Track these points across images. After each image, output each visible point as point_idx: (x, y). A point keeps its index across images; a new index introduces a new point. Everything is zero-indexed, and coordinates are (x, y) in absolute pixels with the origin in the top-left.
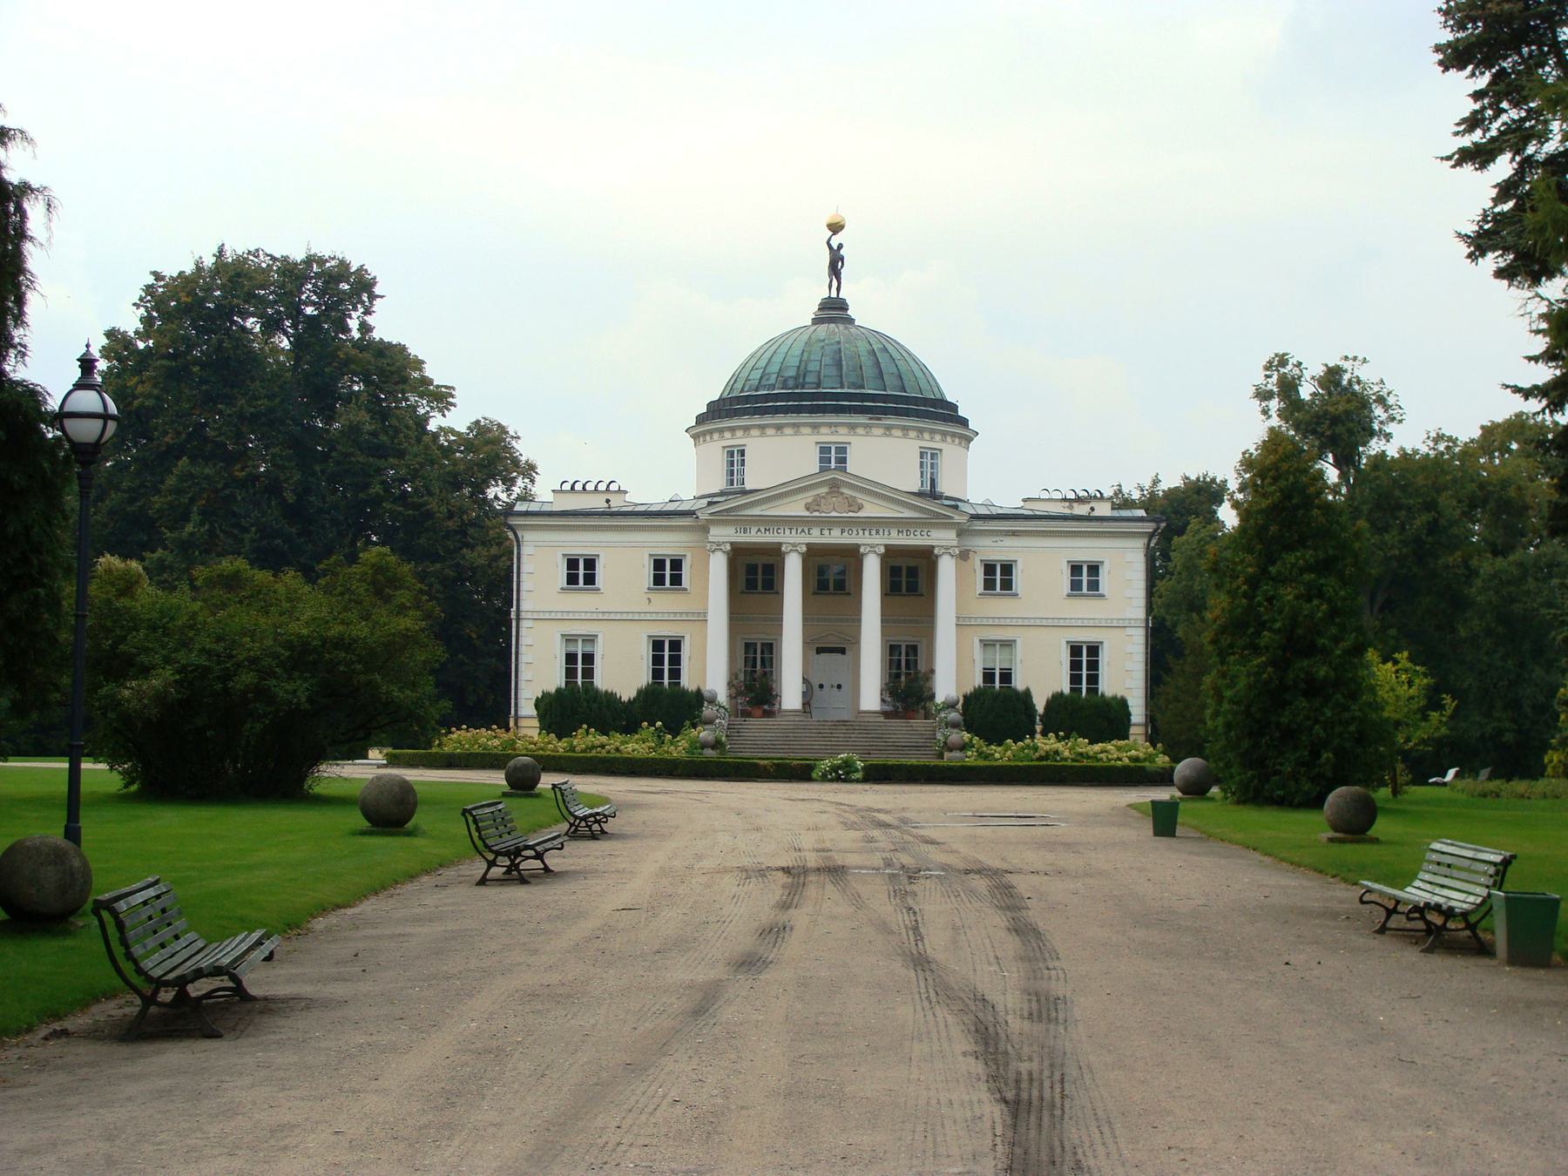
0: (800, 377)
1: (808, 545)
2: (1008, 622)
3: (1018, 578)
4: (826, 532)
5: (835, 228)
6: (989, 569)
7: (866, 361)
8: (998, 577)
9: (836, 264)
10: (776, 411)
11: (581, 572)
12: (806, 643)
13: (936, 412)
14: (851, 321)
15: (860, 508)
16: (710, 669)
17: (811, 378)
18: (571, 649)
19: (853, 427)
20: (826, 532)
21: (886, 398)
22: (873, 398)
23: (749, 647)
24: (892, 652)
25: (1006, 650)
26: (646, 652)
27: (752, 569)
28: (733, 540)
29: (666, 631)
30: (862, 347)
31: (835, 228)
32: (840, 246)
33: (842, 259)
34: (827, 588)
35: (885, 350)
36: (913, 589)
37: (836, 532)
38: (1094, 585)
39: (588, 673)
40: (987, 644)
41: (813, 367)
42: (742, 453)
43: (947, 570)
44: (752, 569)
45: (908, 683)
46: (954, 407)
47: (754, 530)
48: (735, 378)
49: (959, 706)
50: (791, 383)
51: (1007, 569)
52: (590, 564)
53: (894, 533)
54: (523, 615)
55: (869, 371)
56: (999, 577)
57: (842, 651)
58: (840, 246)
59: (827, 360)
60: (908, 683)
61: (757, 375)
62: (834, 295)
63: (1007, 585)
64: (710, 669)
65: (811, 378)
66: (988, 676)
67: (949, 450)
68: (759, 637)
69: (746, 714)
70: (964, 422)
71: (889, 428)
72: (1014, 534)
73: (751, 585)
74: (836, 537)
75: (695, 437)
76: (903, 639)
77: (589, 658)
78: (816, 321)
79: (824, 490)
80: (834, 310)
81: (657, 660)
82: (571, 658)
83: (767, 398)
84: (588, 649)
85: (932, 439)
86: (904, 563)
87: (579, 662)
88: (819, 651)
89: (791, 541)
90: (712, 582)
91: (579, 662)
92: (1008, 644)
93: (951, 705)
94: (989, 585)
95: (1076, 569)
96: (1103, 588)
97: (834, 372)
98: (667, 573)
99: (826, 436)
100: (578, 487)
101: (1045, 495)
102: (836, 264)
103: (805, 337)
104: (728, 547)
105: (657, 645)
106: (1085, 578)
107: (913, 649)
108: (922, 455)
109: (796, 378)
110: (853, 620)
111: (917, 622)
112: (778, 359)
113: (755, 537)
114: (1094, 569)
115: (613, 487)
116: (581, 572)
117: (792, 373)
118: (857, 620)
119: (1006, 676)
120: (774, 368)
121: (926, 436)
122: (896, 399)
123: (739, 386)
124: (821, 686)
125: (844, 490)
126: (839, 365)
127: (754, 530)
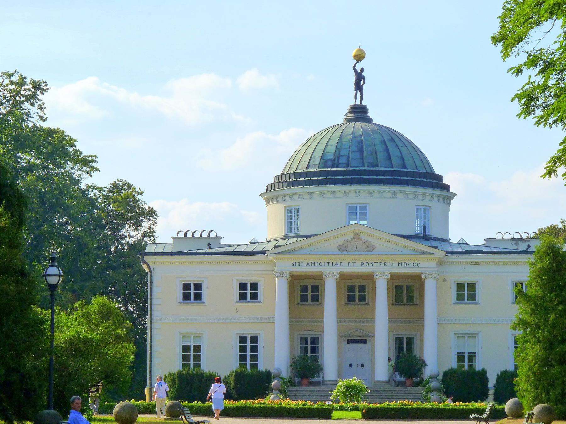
0: (335, 162)
3: (479, 293)
5: (359, 57)
6: (460, 287)
7: (380, 148)
8: (466, 292)
10: (320, 183)
11: (192, 292)
12: (340, 336)
14: (369, 120)
15: (373, 249)
16: (276, 356)
17: (343, 160)
18: (186, 342)
19: (371, 193)
21: (393, 173)
22: (384, 173)
23: (304, 340)
24: (399, 341)
26: (236, 345)
27: (304, 289)
29: (248, 331)
30: (377, 139)
31: (359, 57)
32: (362, 70)
33: (363, 78)
35: (392, 140)
36: (410, 299)
39: (198, 358)
40: (459, 336)
41: (344, 152)
42: (298, 211)
43: (430, 288)
44: (304, 289)
45: (407, 364)
46: (440, 178)
48: (292, 159)
49: (441, 377)
50: (329, 163)
51: (472, 287)
52: (198, 286)
54: (154, 320)
55: (381, 155)
56: (467, 292)
57: (365, 342)
58: (362, 70)
59: (354, 148)
60: (407, 364)
61: (307, 158)
63: (472, 297)
64: (276, 356)
65: (343, 160)
66: (460, 357)
67: (436, 206)
68: (310, 334)
69: (300, 384)
71: (395, 193)
72: (476, 263)
73: (304, 299)
74: (358, 269)
75: (267, 200)
76: (405, 334)
77: (198, 348)
80: (359, 113)
81: (243, 349)
82: (186, 348)
83: (314, 174)
84: (197, 342)
85: (424, 199)
86: (404, 283)
87: (191, 352)
88: (349, 342)
90: (276, 295)
91: (191, 352)
92: (473, 336)
93: (434, 377)
94: (460, 298)
97: (357, 155)
98: (248, 292)
99: (354, 200)
100: (189, 235)
101: (499, 236)
103: (339, 133)
104: (288, 276)
105: (243, 339)
107: (410, 341)
108: (417, 209)
109: (333, 160)
110: (371, 322)
112: (321, 147)
115: (213, 235)
116: (192, 292)
117: (330, 157)
118: (373, 322)
119: (472, 357)
120: (319, 154)
121: (420, 197)
122: (399, 173)
123: (295, 165)
124: (351, 365)
125: (362, 236)
126: (361, 151)
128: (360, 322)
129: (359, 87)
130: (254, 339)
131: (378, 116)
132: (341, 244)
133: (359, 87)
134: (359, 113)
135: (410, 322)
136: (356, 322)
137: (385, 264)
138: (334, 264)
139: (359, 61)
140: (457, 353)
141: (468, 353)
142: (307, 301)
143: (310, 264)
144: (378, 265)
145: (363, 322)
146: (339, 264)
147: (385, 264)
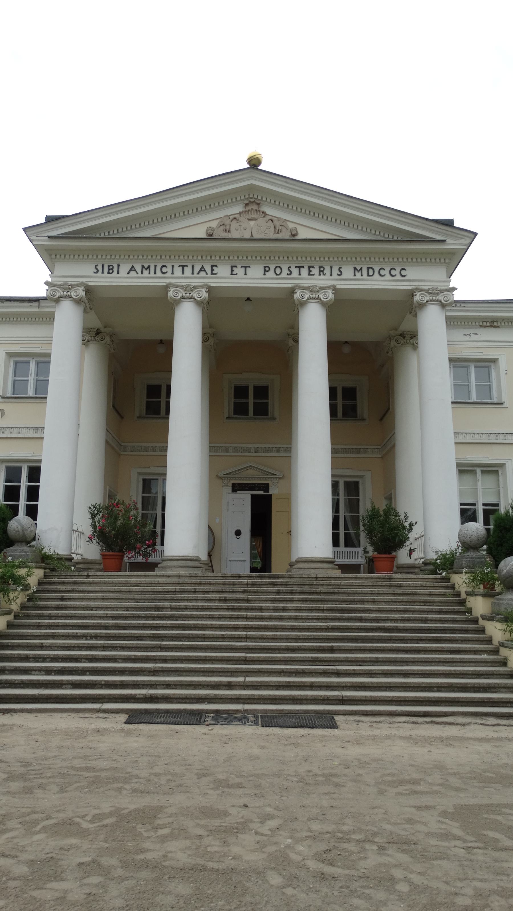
1: (210, 290)
2: (493, 439)
4: (240, 271)
20: (240, 271)
25: (490, 479)
28: (93, 282)
34: (246, 413)
37: (256, 270)
47: (125, 268)
53: (348, 272)
74: (255, 278)
79: (237, 209)
88: (236, 488)
89: (183, 282)
92: (493, 470)
104: (81, 293)
110: (278, 450)
111: (358, 451)
113: (127, 278)
124: (238, 533)
127: (125, 268)
128: (257, 450)
130: (35, 473)
132: (214, 224)
135: (351, 451)
136: (249, 450)
137: (321, 271)
138: (196, 270)
140: (461, 504)
141: (484, 505)
142: (159, 414)
143: (139, 268)
144: (305, 272)
145: (264, 450)
146: (208, 270)
147: (321, 271)
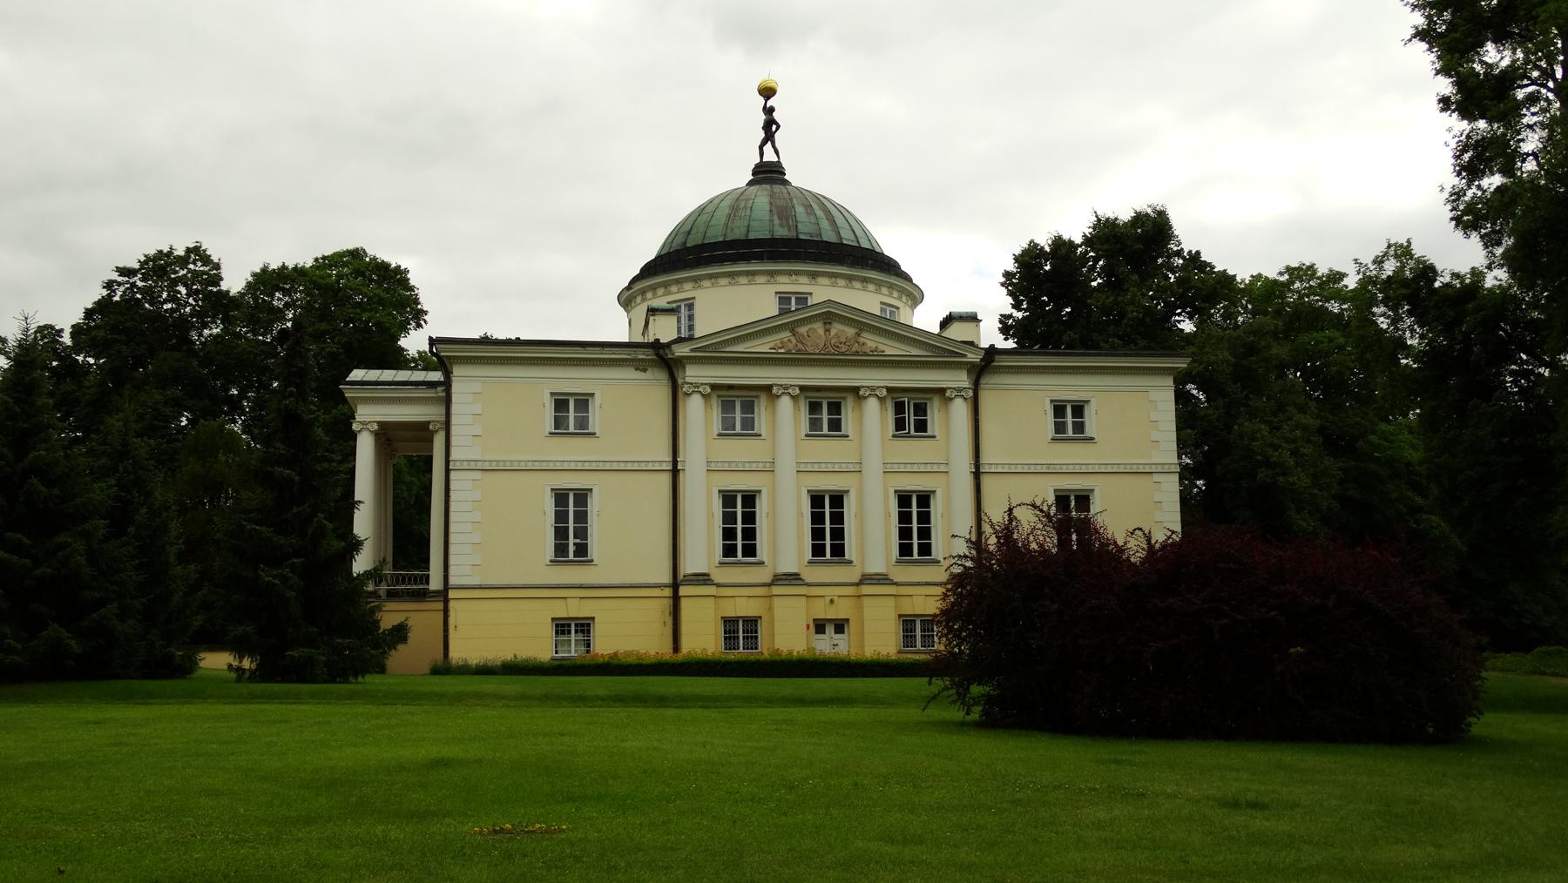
5: (767, 92)
9: (770, 127)
13: (888, 266)
14: (786, 183)
31: (767, 92)
38: (1079, 428)
42: (691, 307)
58: (772, 110)
62: (769, 156)
70: (907, 278)
78: (750, 183)
80: (768, 173)
95: (1059, 410)
96: (1090, 430)
102: (770, 127)
106: (1069, 419)
114: (1079, 410)
123: (680, 240)
129: (769, 136)
131: (796, 175)
133: (769, 136)
134: (768, 173)
139: (767, 98)
